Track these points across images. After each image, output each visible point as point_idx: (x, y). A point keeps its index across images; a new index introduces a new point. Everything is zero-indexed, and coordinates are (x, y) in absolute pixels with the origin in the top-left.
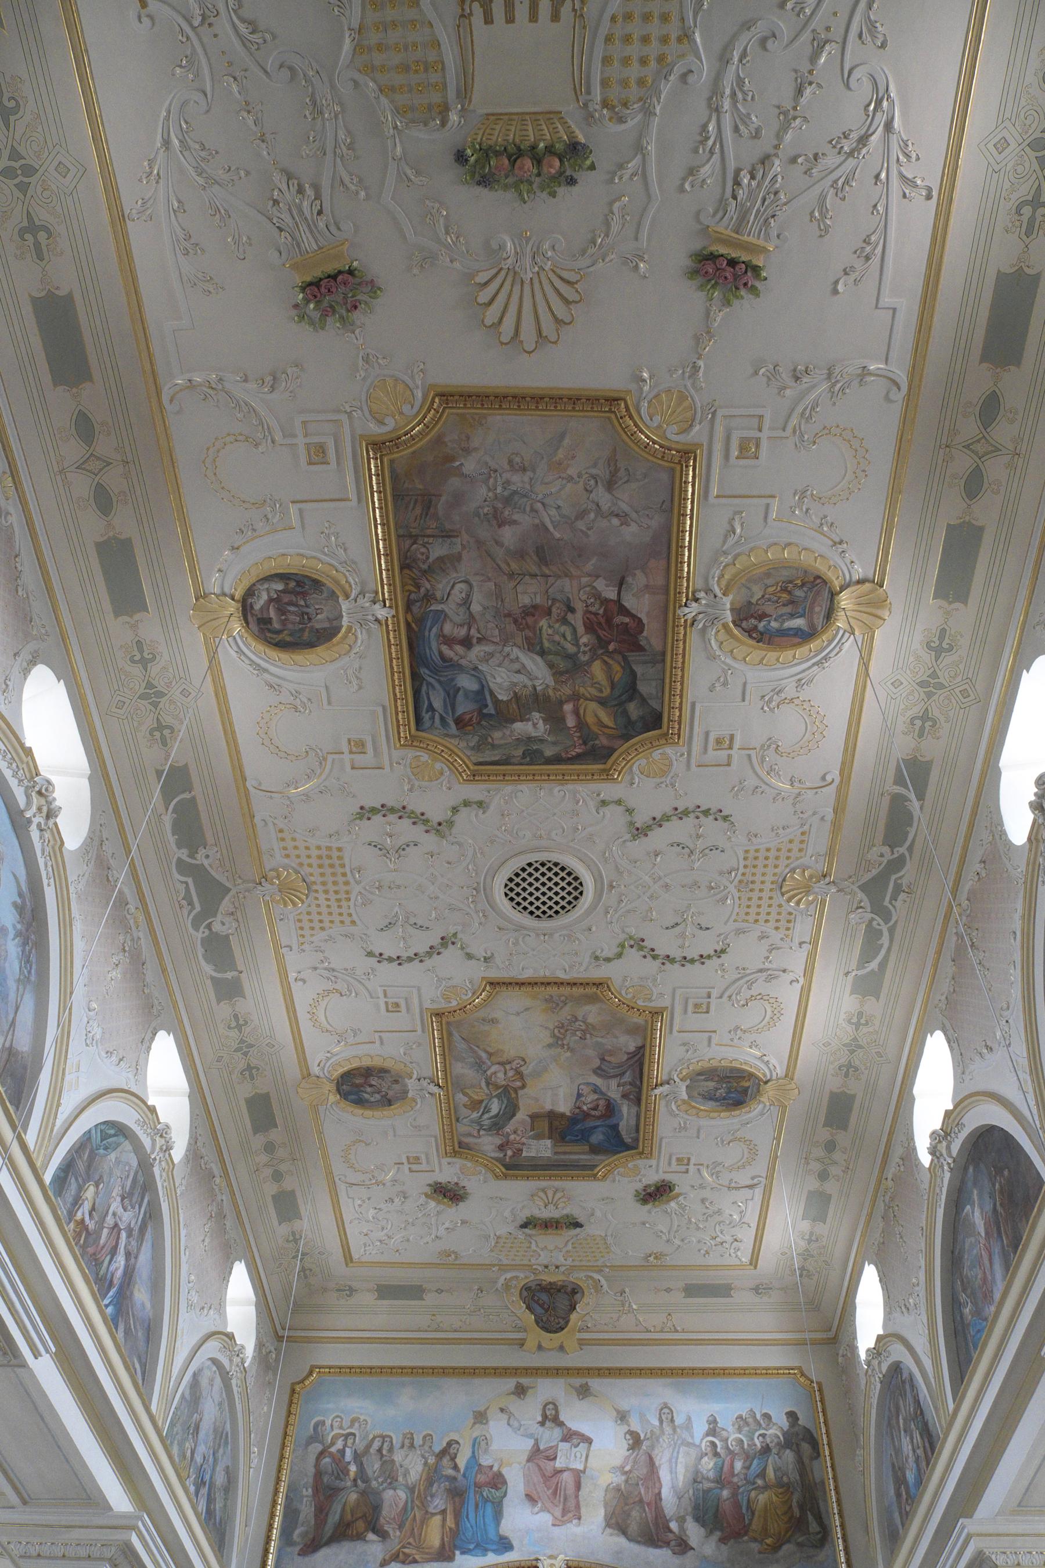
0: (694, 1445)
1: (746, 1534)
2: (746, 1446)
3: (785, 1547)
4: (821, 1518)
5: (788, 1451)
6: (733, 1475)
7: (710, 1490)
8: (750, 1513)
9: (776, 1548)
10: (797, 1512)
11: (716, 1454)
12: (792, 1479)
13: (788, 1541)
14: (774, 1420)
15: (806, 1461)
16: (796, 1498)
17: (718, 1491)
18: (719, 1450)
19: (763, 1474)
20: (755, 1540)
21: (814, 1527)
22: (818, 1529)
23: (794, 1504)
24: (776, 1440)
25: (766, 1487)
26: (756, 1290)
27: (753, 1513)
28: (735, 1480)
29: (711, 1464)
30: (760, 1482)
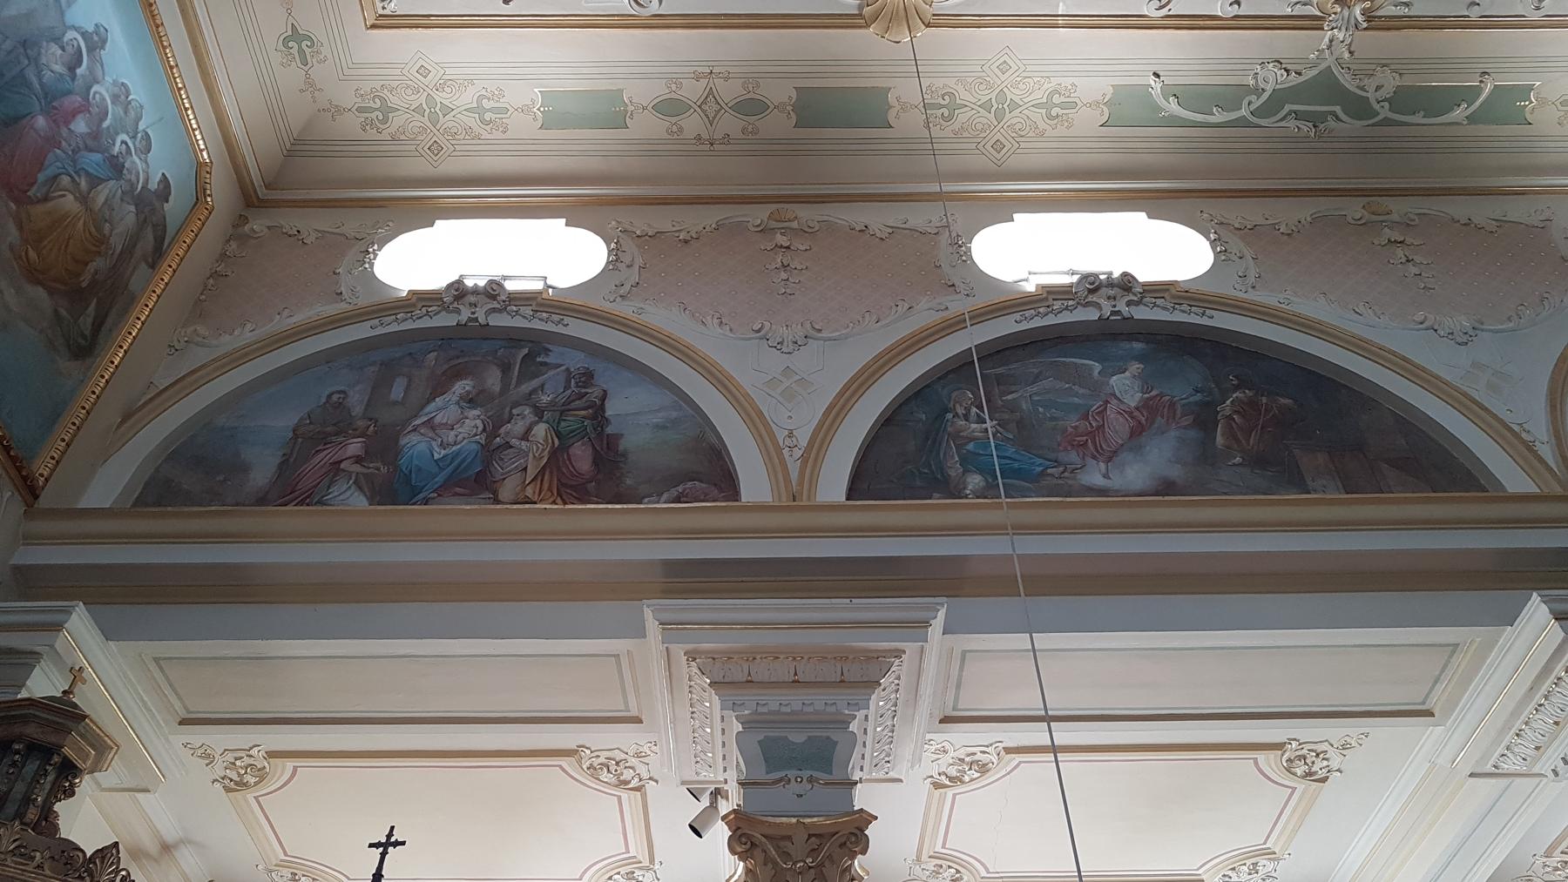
0: (62, 14)
1: (16, 201)
2: (106, 124)
3: (40, 292)
4: (102, 323)
5: (132, 208)
6: (67, 123)
7: (28, 85)
8: (44, 190)
9: (34, 275)
10: (85, 280)
11: (72, 69)
12: (112, 240)
13: (51, 292)
14: (149, 155)
15: (138, 252)
16: (98, 264)
17: (38, 108)
18: (79, 71)
19: (95, 182)
20: (20, 228)
21: (86, 322)
22: (87, 333)
23: (92, 267)
24: (133, 178)
25: (84, 199)
26: (295, 35)
27: (46, 199)
28: (64, 132)
29: (58, 68)
30: (83, 184)
